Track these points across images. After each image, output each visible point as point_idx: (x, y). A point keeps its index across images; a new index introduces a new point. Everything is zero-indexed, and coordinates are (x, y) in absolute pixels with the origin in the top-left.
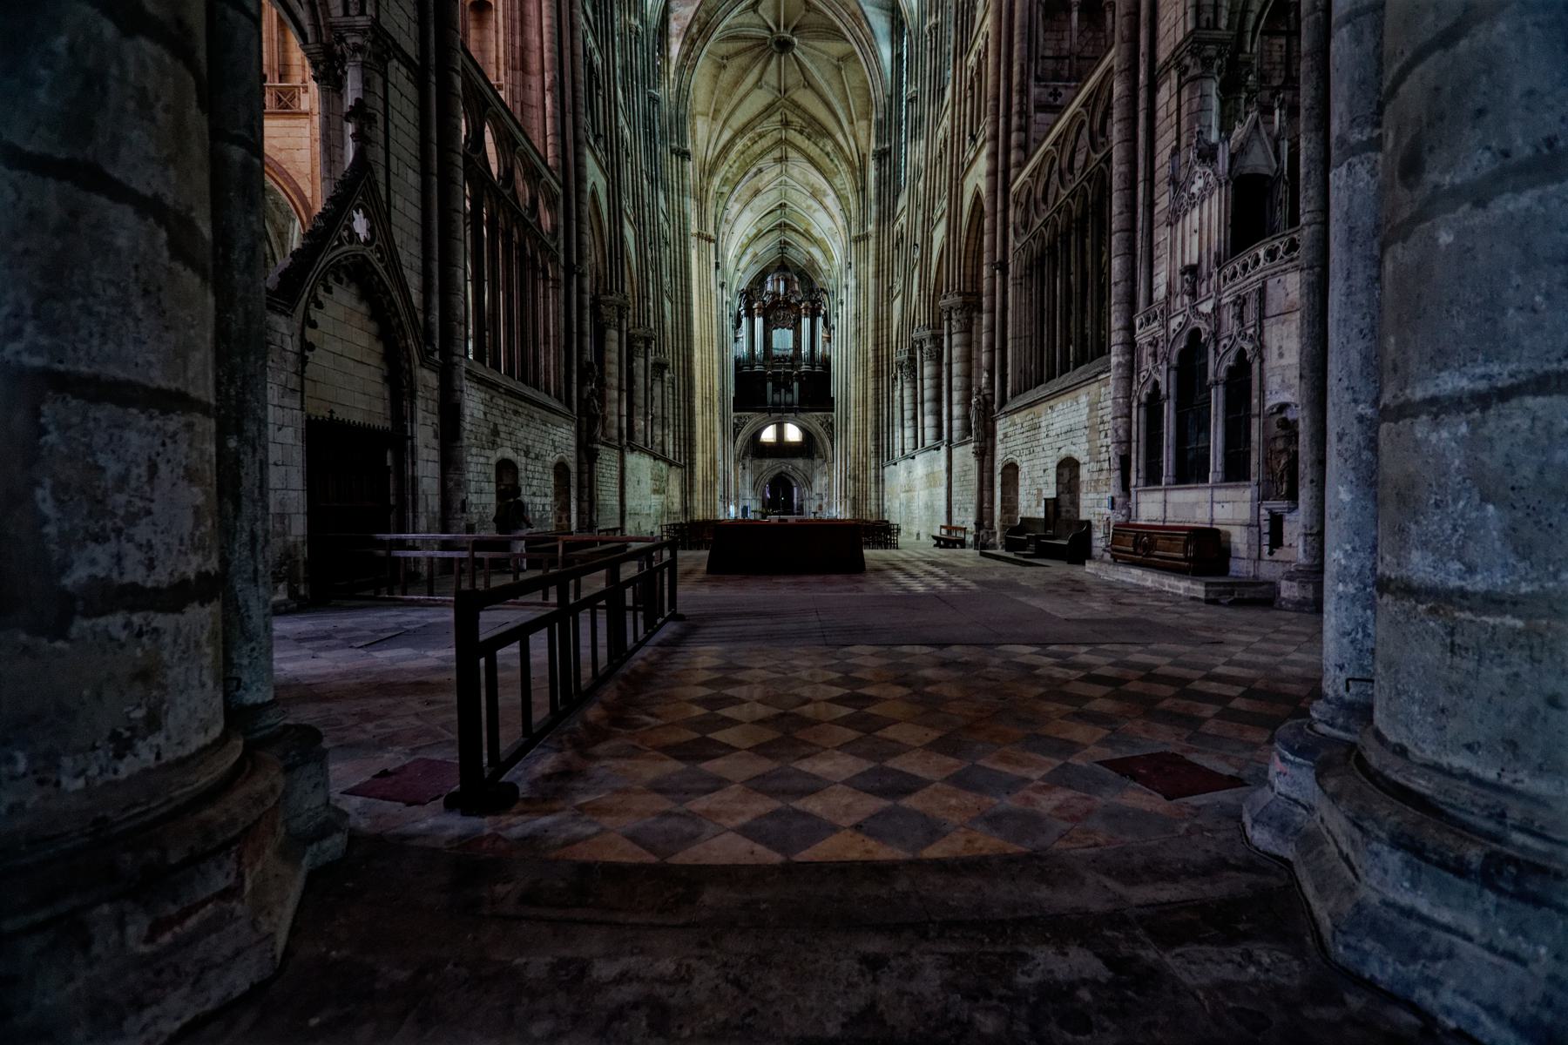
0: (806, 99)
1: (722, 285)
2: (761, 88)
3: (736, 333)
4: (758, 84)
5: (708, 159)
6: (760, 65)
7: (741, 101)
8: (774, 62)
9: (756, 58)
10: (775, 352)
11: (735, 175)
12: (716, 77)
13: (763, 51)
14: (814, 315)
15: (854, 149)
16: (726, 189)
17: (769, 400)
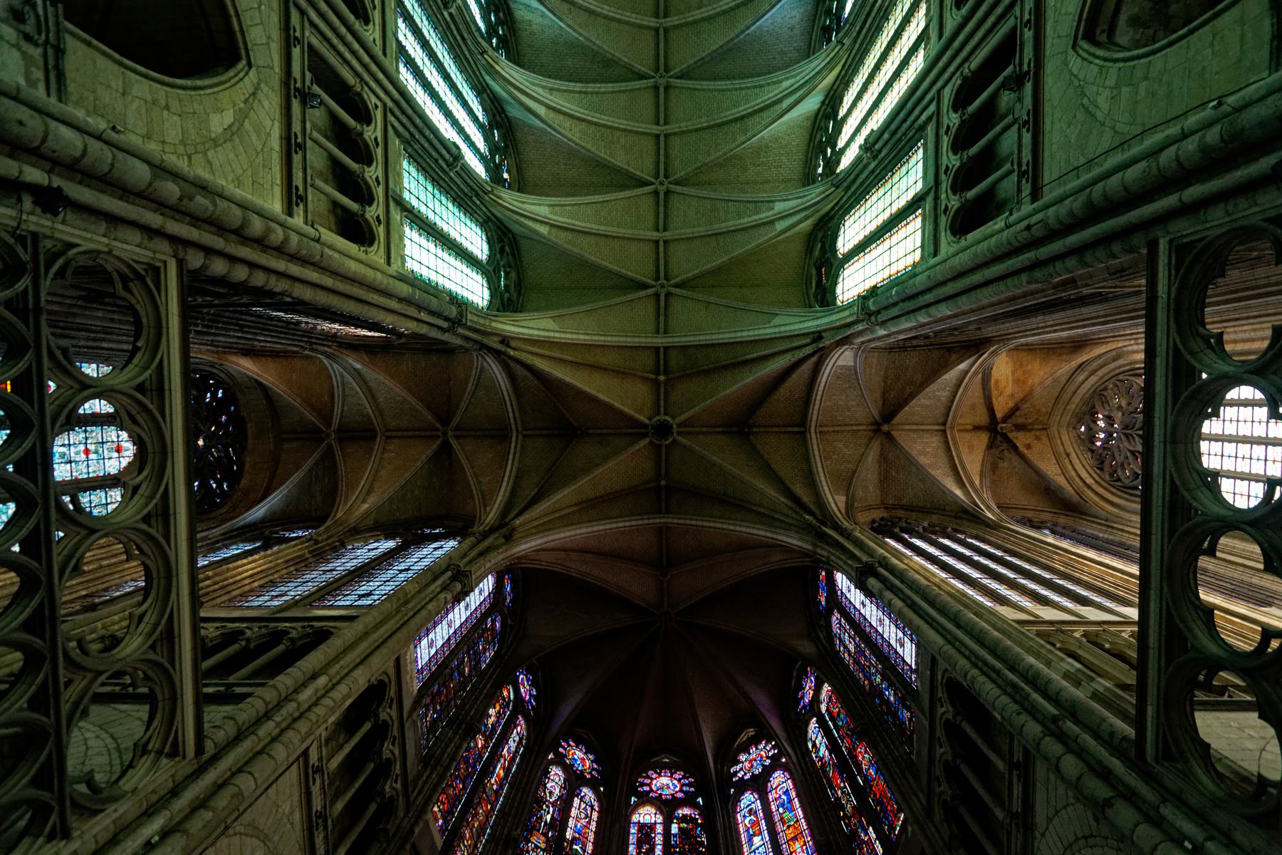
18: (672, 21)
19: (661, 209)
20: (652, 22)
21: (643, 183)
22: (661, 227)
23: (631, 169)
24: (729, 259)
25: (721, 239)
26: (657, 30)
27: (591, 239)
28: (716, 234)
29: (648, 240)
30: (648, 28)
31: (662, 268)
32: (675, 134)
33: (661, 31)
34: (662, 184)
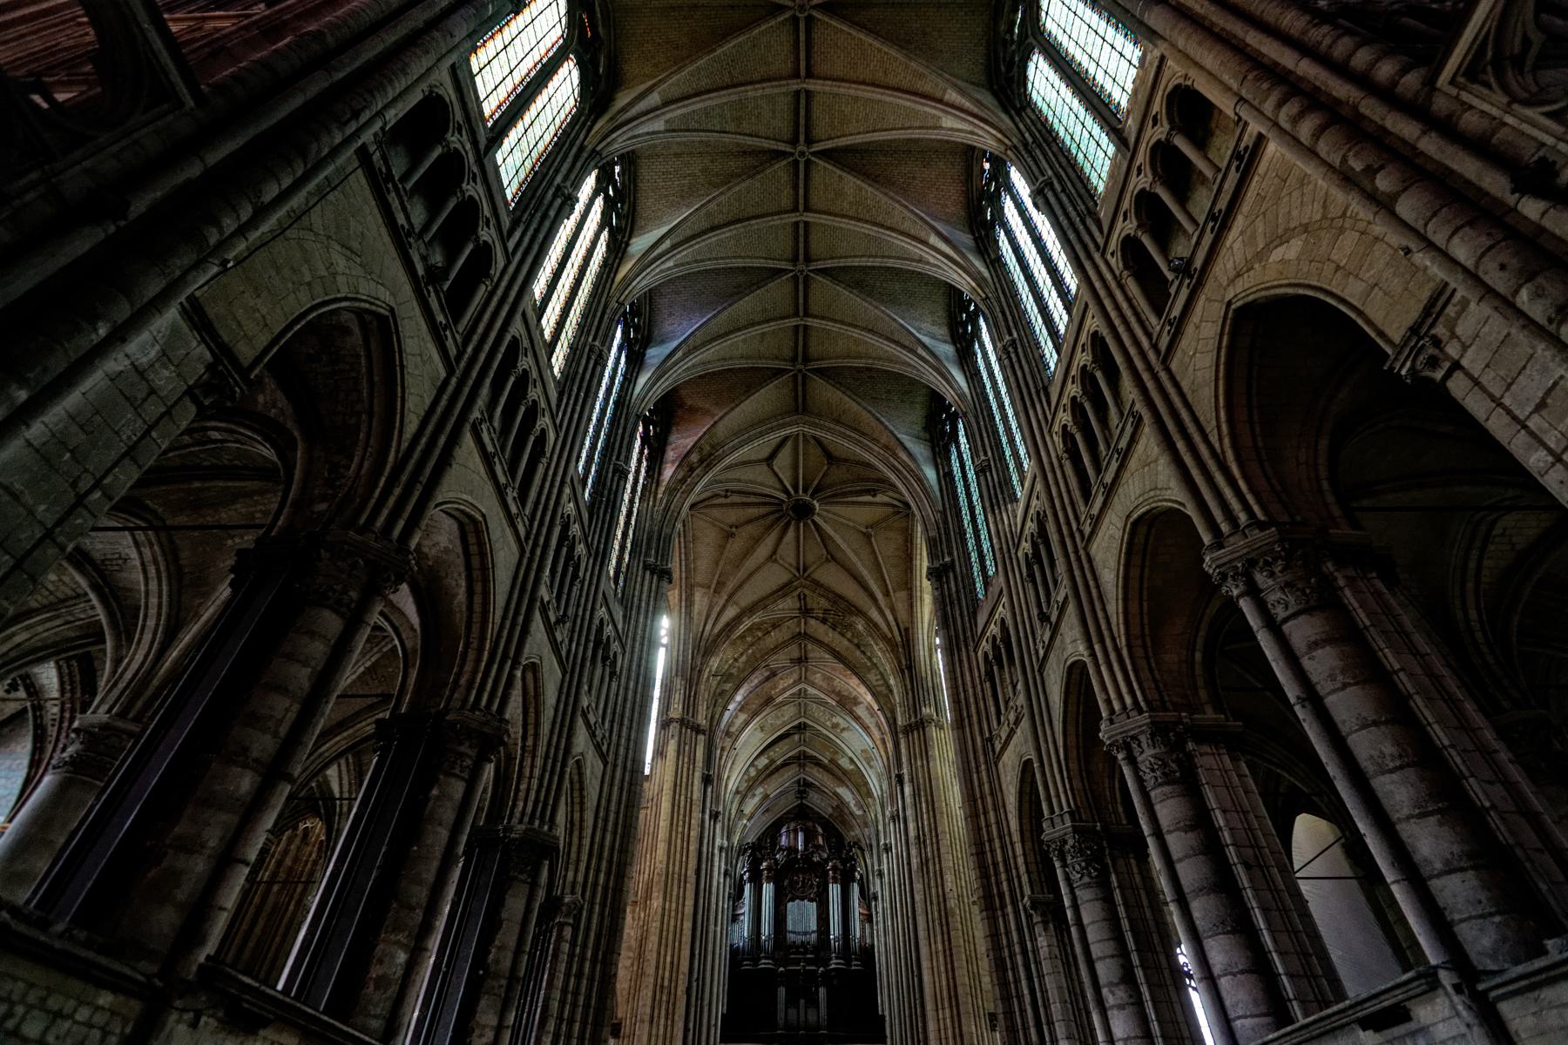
0: (830, 576)
1: (715, 816)
2: (776, 561)
3: (735, 908)
4: (772, 557)
5: (706, 633)
6: (774, 535)
7: (751, 575)
8: (791, 534)
9: (769, 528)
10: (791, 937)
11: (741, 671)
12: (722, 548)
13: (778, 519)
14: (846, 881)
15: (893, 623)
16: (728, 686)
17: (781, 1022)
18: (794, 322)
19: (802, 121)
20: (810, 322)
21: (826, 154)
22: (803, 96)
23: (838, 172)
24: (714, 50)
25: (727, 80)
26: (807, 314)
27: (893, 81)
28: (734, 86)
29: (819, 78)
30: (816, 317)
31: (802, 37)
32: (786, 212)
33: (801, 313)
34: (802, 154)
